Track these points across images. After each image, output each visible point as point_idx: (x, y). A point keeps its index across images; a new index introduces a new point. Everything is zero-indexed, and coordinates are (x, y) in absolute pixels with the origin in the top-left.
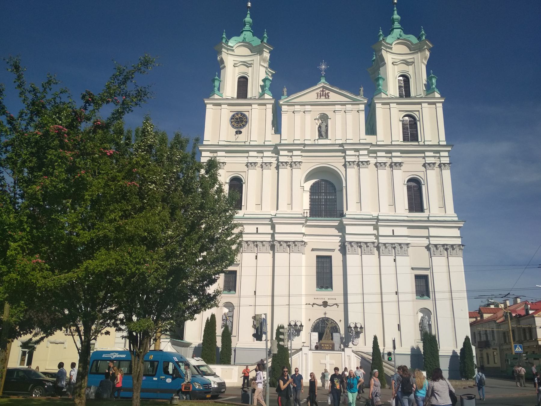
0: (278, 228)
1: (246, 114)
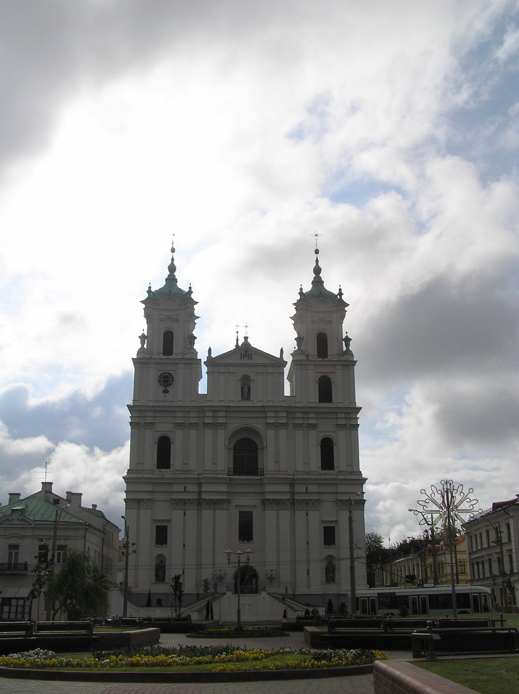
0: (205, 488)
1: (172, 373)
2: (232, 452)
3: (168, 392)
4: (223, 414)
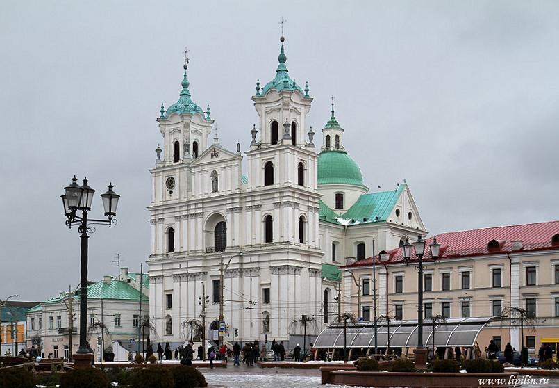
4: (200, 206)
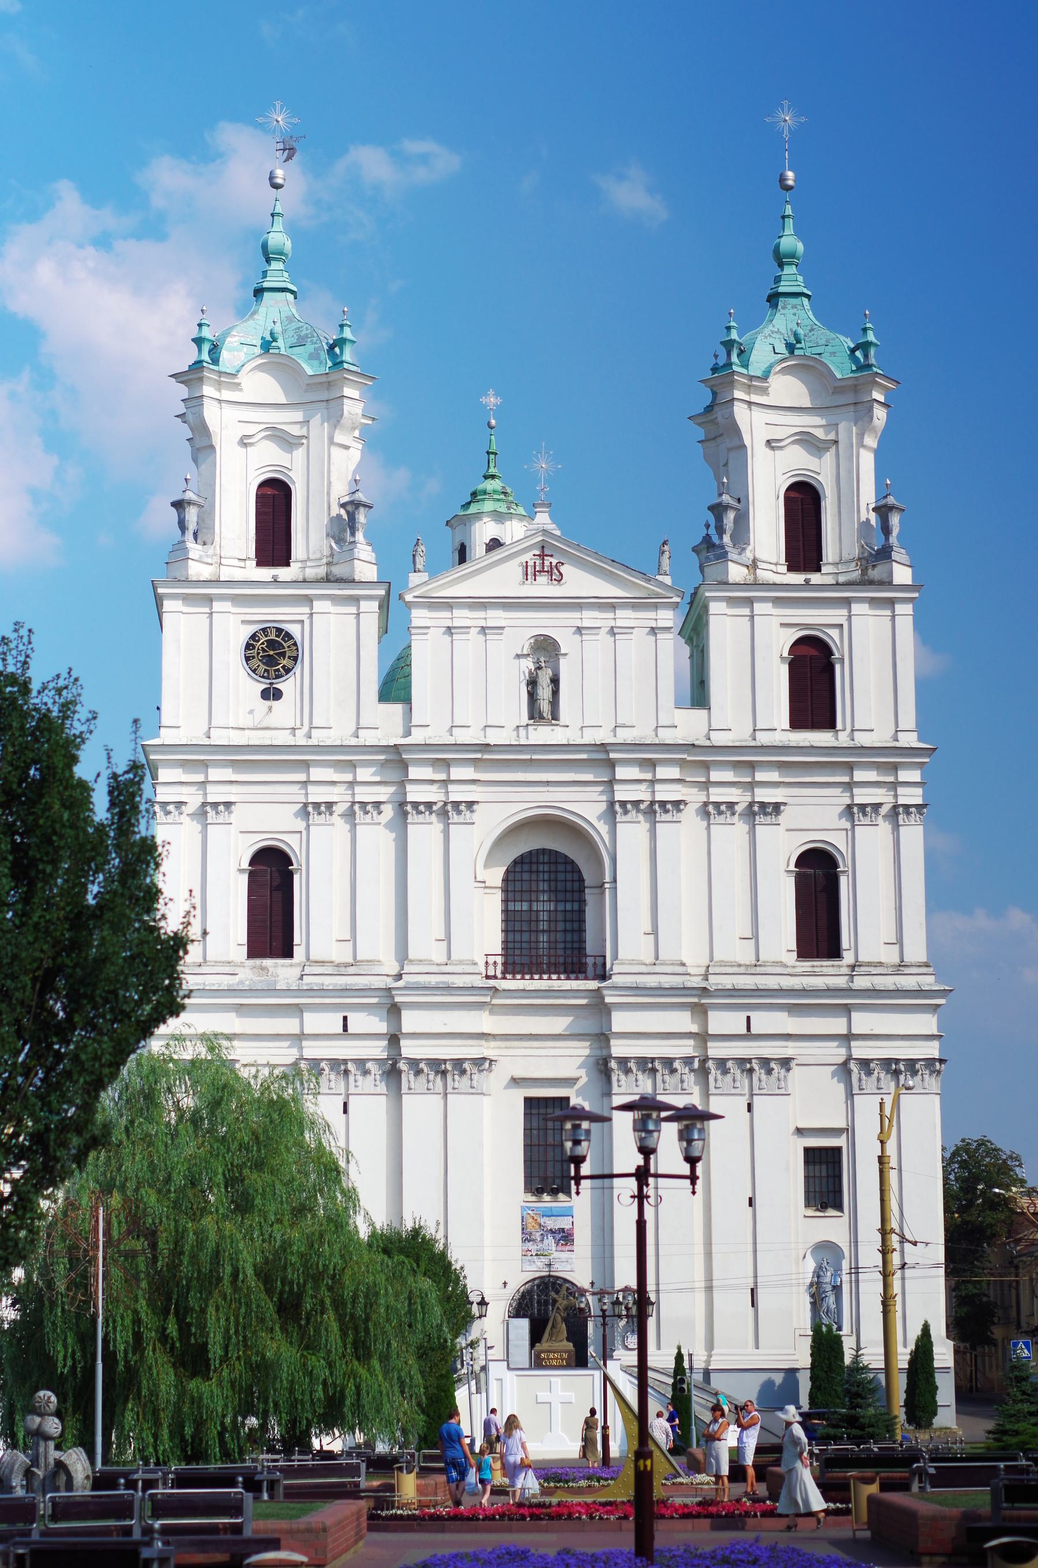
0: (410, 1022)
1: (294, 630)
2: (498, 896)
3: (278, 695)
